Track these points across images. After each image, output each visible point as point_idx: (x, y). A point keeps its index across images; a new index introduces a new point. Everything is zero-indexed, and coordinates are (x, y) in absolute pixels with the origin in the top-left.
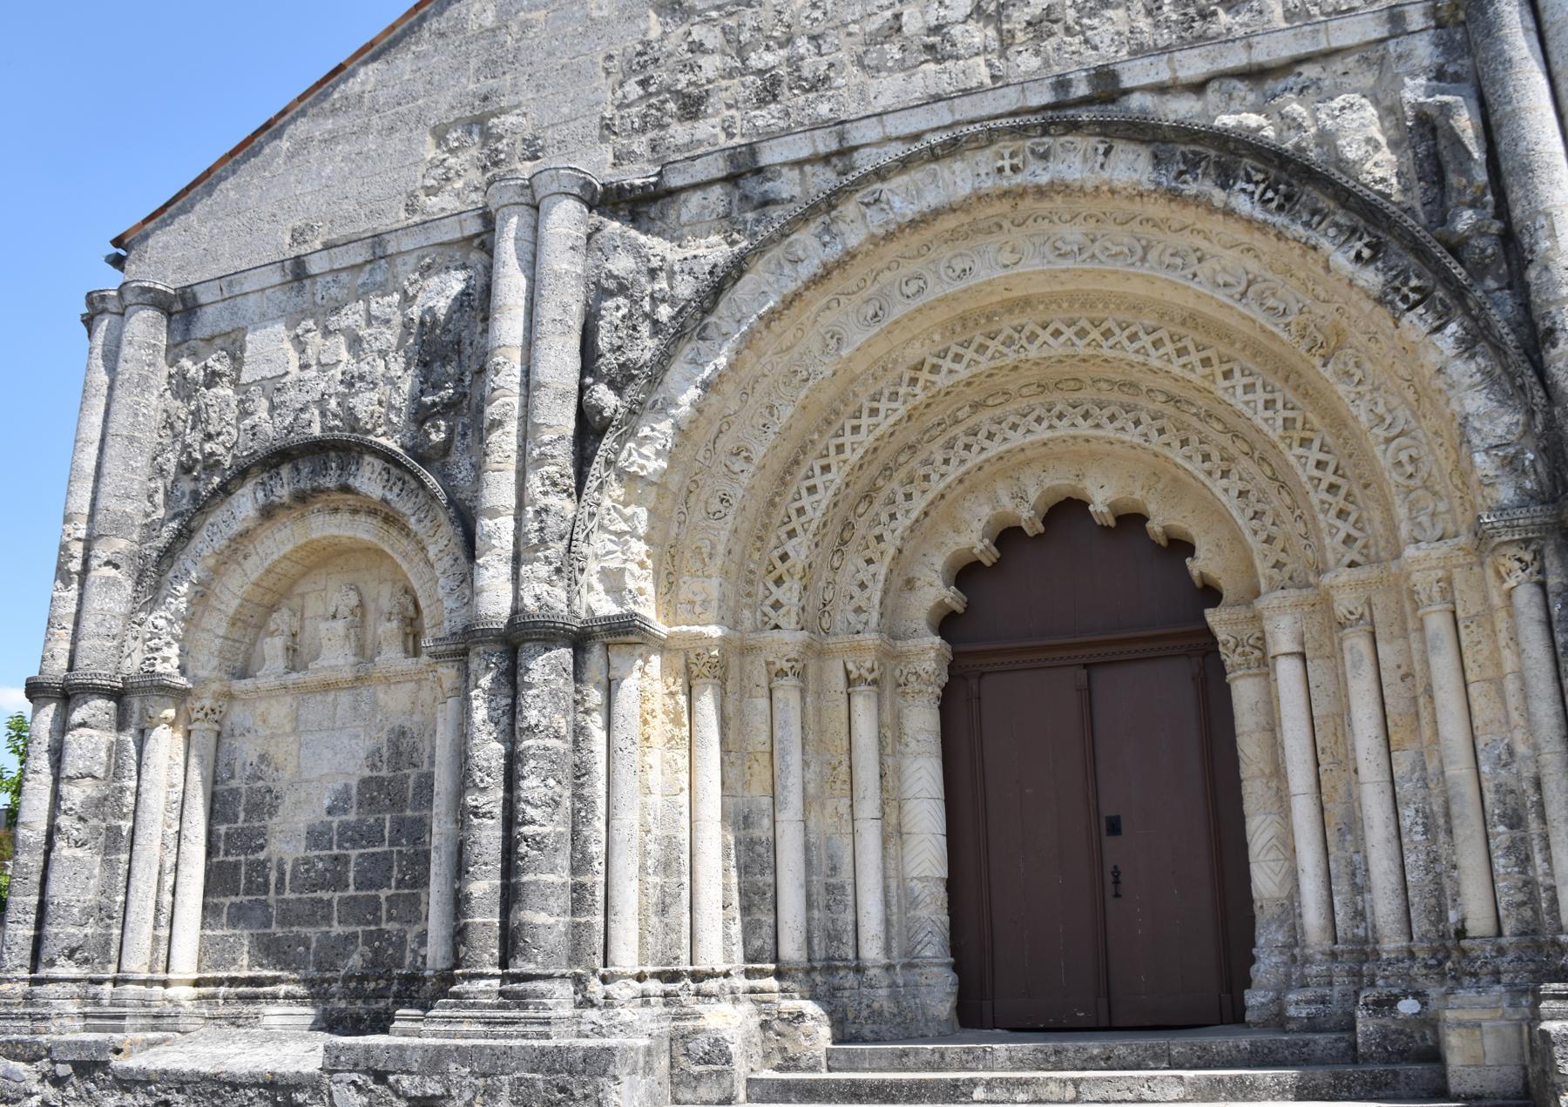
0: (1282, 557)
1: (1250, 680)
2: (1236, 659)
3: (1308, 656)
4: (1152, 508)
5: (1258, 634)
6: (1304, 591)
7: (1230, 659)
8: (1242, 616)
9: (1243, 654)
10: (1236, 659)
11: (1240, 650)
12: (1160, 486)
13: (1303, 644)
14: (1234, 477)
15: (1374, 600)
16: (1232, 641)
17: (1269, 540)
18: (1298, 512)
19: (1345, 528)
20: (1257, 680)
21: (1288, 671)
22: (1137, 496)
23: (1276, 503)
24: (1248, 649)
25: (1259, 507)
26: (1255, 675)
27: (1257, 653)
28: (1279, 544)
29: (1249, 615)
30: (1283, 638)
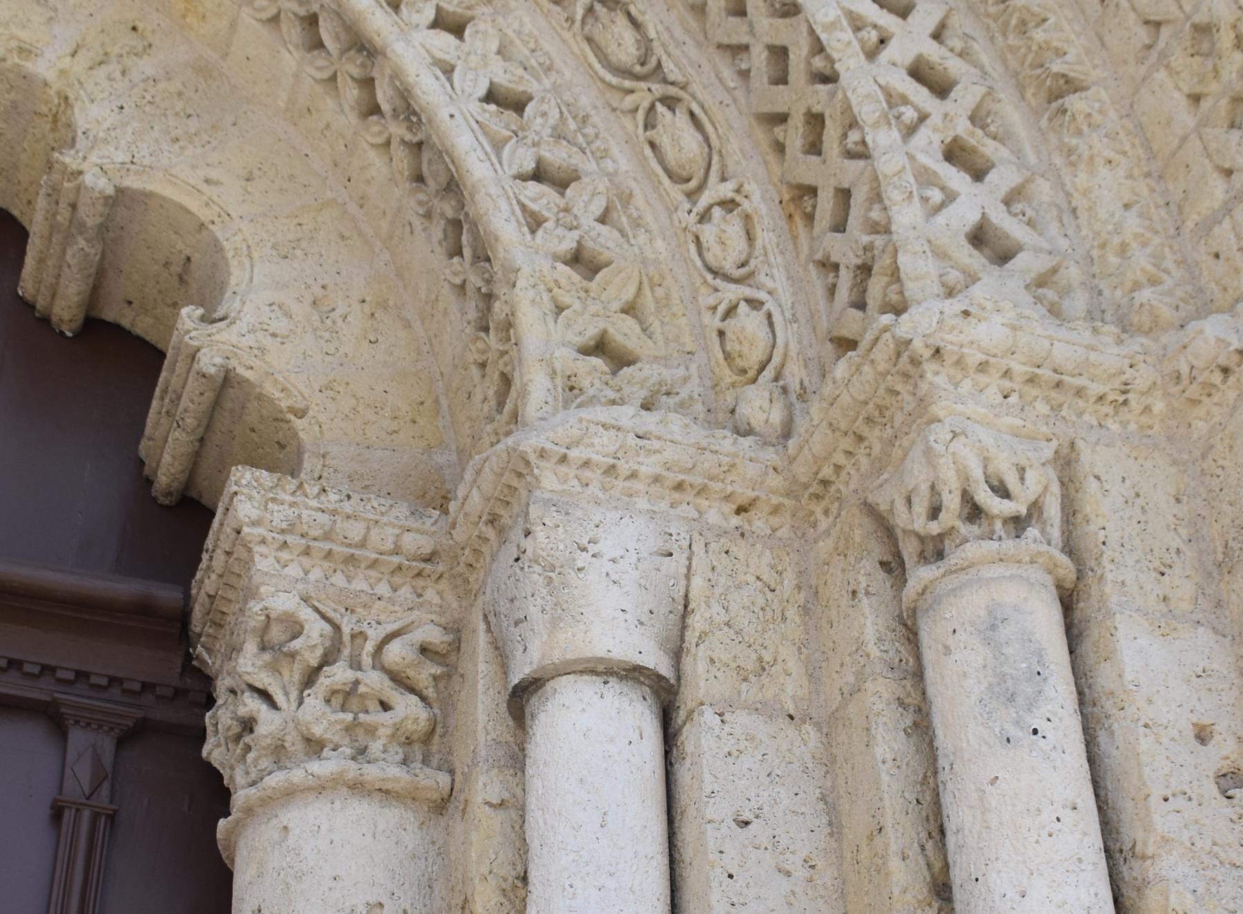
0: (625, 332)
1: (361, 809)
2: (316, 714)
3: (688, 698)
4: (91, 115)
5: (433, 635)
6: (726, 442)
7: (264, 716)
8: (382, 538)
9: (346, 696)
10: (316, 714)
11: (339, 674)
12: (146, 66)
13: (677, 655)
14: (482, 37)
15: (1091, 458)
16: (316, 630)
17: (582, 261)
18: (717, 190)
19: (972, 203)
20: (390, 816)
21: (592, 746)
22: (43, 68)
23: (622, 162)
24: (374, 681)
25: (558, 156)
26: (386, 794)
27: (408, 709)
28: (616, 286)
29: (417, 542)
30: (601, 582)
